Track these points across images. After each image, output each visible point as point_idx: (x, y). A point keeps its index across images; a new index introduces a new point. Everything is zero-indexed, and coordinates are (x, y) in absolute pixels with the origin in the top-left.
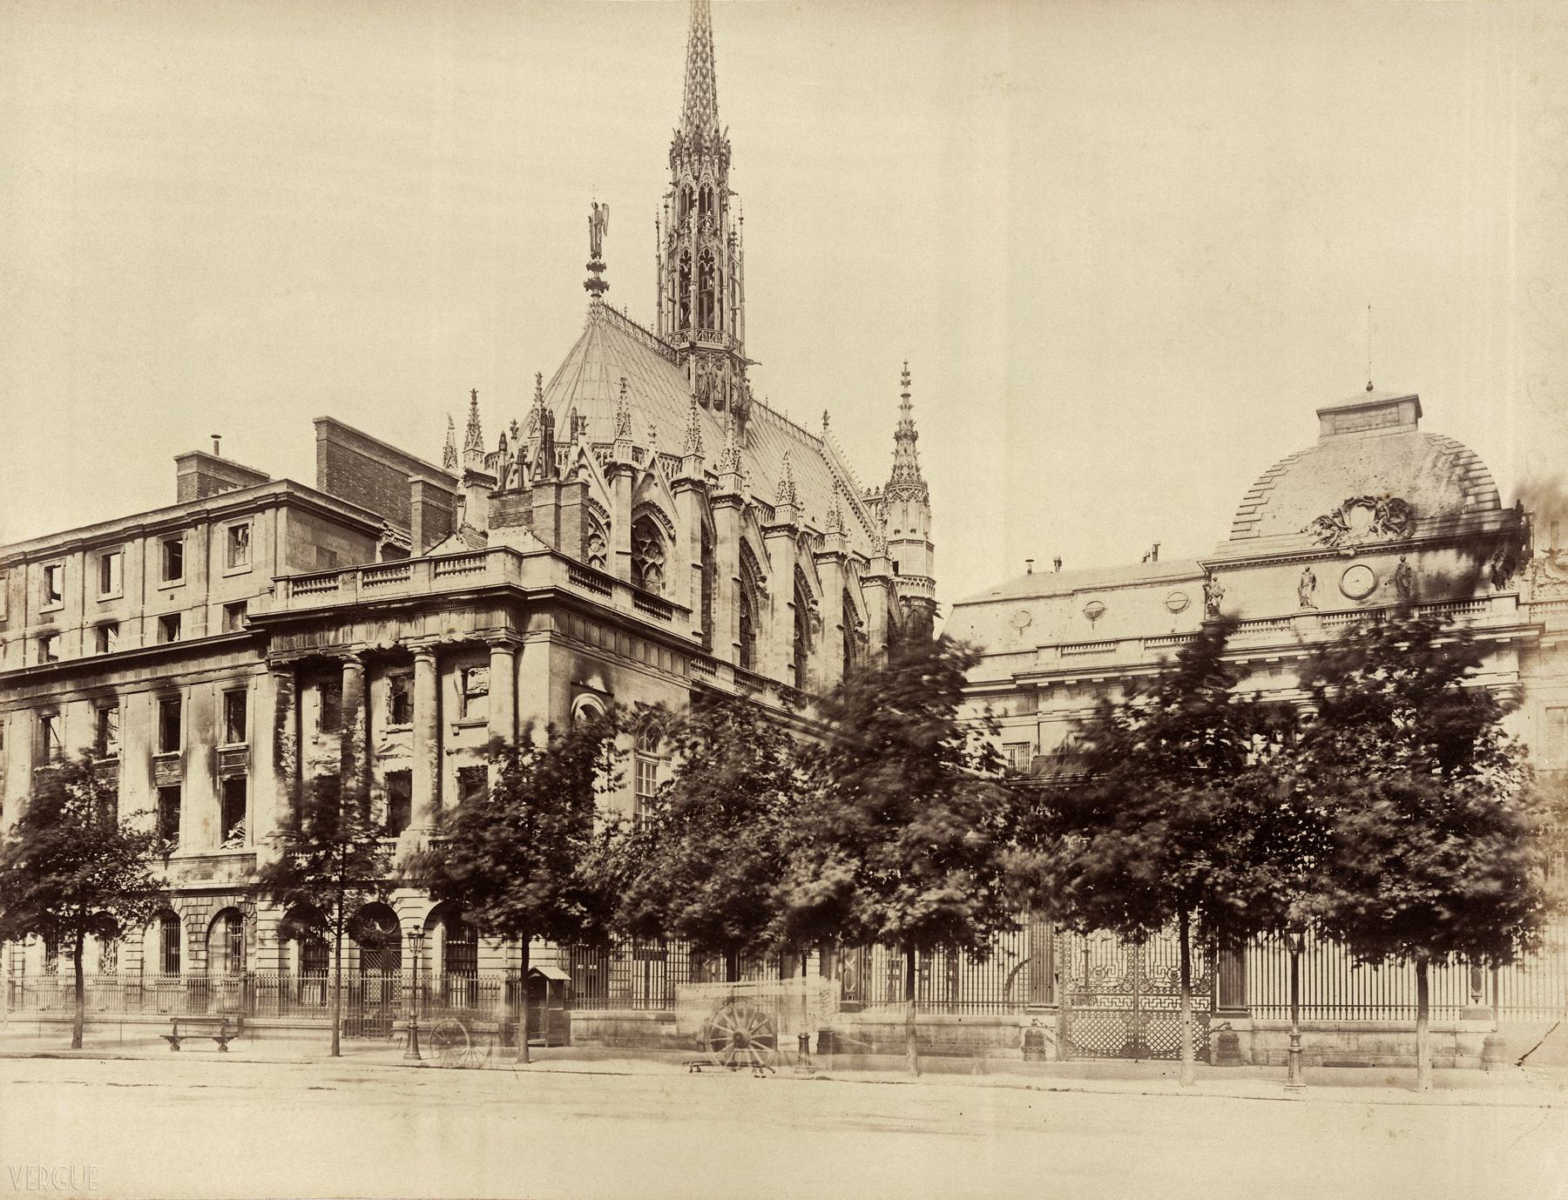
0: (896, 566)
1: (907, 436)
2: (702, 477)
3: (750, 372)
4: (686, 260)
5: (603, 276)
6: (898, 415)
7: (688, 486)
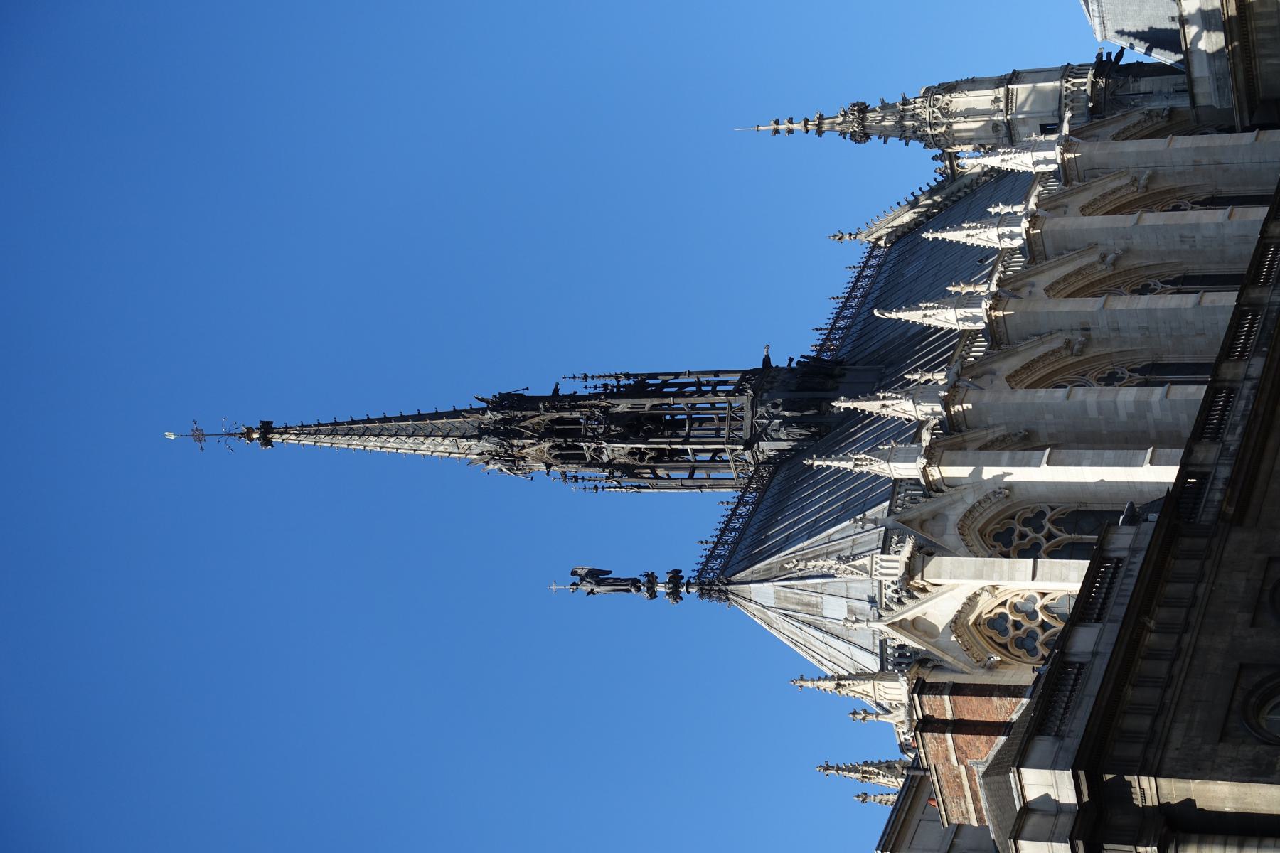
3: (779, 361)
5: (663, 577)
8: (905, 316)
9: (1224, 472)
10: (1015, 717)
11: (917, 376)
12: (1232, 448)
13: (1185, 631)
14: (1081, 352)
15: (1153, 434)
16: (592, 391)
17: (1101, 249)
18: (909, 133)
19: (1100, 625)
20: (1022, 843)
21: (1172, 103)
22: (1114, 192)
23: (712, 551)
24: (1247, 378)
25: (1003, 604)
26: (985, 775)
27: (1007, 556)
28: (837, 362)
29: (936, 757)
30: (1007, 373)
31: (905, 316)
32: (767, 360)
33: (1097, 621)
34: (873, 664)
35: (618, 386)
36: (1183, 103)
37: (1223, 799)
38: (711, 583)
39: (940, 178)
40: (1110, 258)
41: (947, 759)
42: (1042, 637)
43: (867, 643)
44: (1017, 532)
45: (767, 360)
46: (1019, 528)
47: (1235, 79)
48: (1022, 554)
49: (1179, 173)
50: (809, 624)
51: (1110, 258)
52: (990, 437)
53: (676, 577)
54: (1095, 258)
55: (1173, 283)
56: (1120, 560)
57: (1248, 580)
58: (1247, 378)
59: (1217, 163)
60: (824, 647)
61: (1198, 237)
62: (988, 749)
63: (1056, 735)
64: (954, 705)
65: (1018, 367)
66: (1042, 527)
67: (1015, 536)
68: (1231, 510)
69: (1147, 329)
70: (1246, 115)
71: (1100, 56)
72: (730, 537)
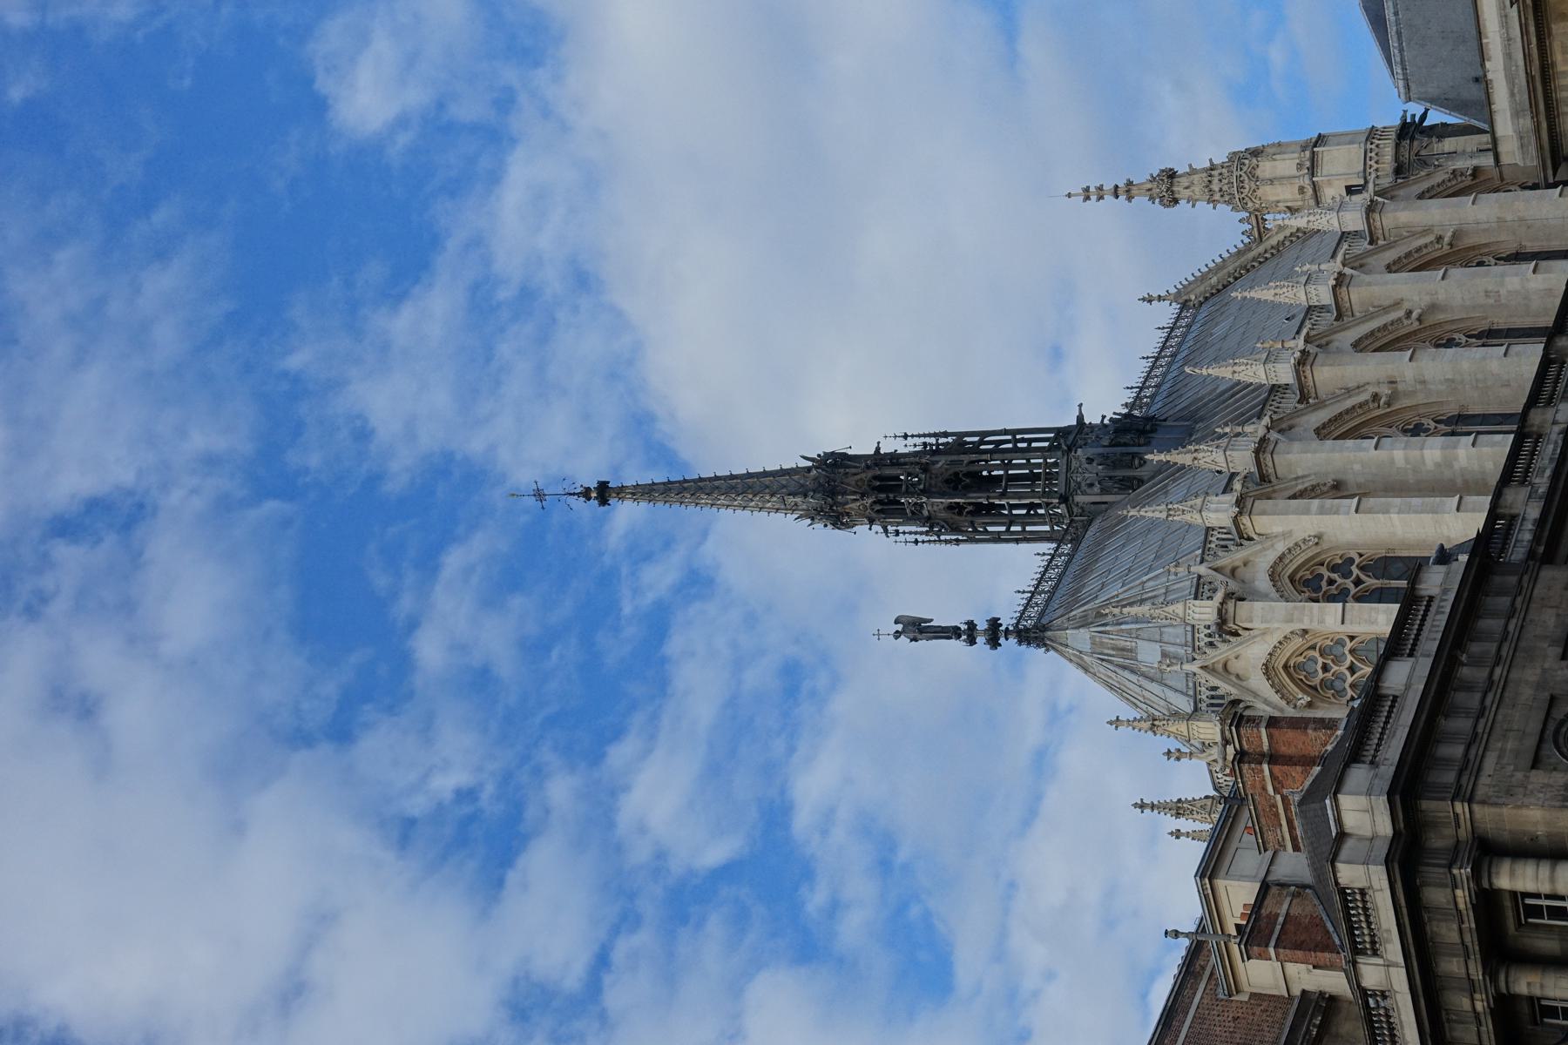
0: (1350, 190)
1: (1167, 187)
2: (1230, 498)
3: (1092, 418)
4: (957, 509)
5: (982, 625)
6: (1141, 201)
7: (1245, 520)
8: (1214, 371)
9: (1534, 512)
10: (1329, 748)
11: (1227, 430)
12: (1542, 490)
13: (1497, 664)
15: (1459, 481)
16: (912, 449)
17: (1406, 306)
18: (1217, 197)
19: (1412, 659)
20: (1339, 866)
21: (1475, 162)
22: (1419, 250)
23: (1030, 599)
24: (1555, 423)
25: (1313, 647)
26: (1301, 803)
27: (1316, 600)
28: (1149, 419)
29: (1253, 786)
31: (1214, 371)
32: (1080, 418)
33: (1411, 655)
34: (1185, 705)
35: (938, 445)
36: (1487, 161)
37: (1536, 824)
38: (1027, 630)
39: (1247, 240)
40: (1415, 315)
41: (1264, 788)
42: (1350, 679)
43: (1181, 685)
45: (1080, 418)
46: (1327, 574)
47: (1539, 138)
48: (1331, 599)
49: (1485, 230)
50: (1124, 668)
51: (1415, 315)
52: (1300, 487)
53: (994, 624)
54: (1401, 313)
55: (1478, 336)
56: (1431, 598)
57: (1558, 615)
58: (1555, 423)
59: (1521, 220)
60: (1138, 690)
61: (1503, 292)
62: (1301, 781)
63: (1372, 763)
64: (1270, 737)
66: (1351, 573)
67: (1324, 583)
68: (1541, 549)
69: (1453, 381)
70: (1550, 172)
71: (1404, 117)
72: (1046, 586)
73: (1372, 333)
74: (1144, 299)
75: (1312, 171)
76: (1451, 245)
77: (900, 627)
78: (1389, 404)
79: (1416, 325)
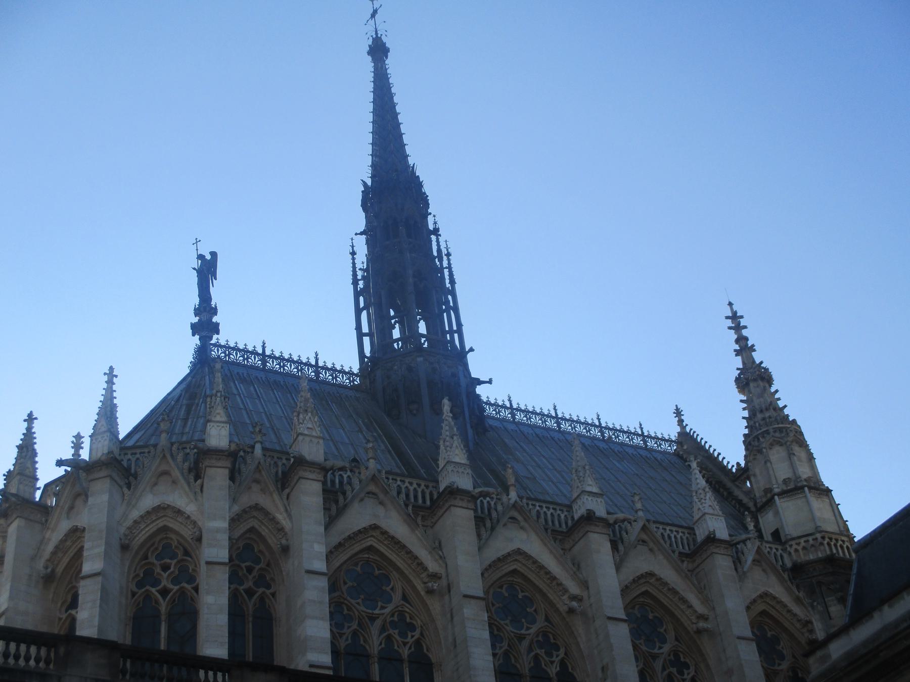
0: (776, 535)
1: (754, 380)
6: (738, 362)
14: (430, 592)
22: (684, 600)
30: (384, 524)
44: (168, 561)
52: (281, 517)
65: (392, 532)
69: (455, 646)
73: (542, 567)
74: (677, 409)
75: (782, 494)
76: (699, 632)
77: (208, 257)
78: (430, 592)
79: (563, 609)
